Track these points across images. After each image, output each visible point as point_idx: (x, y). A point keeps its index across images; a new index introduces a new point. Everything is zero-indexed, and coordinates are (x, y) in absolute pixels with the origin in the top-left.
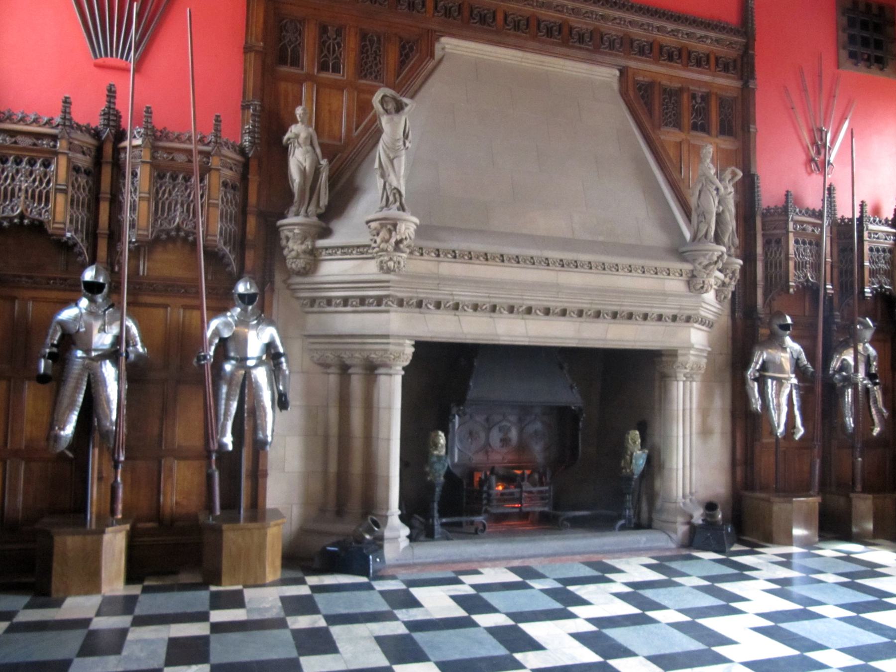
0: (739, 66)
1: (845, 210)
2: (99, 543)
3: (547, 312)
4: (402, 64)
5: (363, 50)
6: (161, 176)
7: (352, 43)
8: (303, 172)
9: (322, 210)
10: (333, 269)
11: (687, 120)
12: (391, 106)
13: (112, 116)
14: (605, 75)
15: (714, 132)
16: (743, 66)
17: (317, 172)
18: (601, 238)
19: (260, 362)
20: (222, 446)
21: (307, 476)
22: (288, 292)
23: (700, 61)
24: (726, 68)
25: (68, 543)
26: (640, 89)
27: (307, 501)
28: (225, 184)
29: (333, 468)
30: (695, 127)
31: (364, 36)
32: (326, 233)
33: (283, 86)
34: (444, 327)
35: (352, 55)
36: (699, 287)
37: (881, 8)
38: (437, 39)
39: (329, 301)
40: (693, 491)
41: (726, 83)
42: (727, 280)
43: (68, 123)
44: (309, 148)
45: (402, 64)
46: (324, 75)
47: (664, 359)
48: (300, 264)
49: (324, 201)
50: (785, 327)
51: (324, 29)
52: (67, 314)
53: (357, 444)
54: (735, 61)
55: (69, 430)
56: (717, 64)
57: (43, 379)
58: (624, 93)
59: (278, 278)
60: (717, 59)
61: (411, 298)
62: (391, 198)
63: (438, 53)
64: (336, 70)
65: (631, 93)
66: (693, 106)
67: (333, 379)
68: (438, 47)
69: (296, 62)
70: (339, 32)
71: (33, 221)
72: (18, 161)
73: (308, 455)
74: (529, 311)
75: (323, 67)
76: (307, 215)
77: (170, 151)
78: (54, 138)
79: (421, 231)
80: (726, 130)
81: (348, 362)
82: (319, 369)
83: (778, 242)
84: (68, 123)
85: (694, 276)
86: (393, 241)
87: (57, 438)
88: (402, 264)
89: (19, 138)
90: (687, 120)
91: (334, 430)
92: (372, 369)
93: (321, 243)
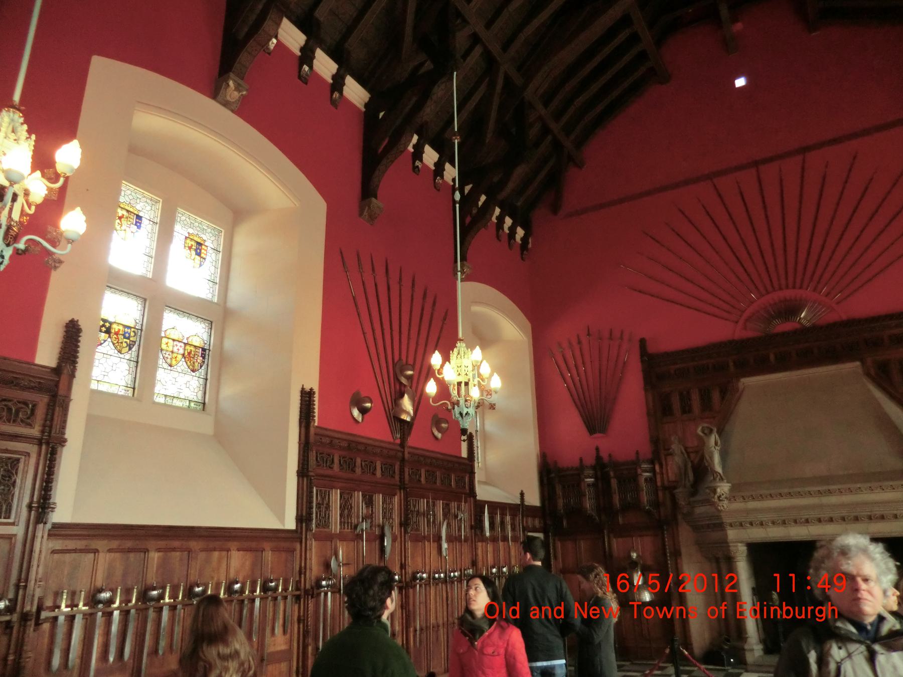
3: (820, 520)
7: (695, 398)
13: (598, 458)
14: (852, 367)
17: (686, 466)
32: (694, 493)
34: (759, 534)
48: (685, 511)
59: (680, 517)
65: (872, 372)
74: (807, 521)
79: (732, 489)
93: (692, 499)
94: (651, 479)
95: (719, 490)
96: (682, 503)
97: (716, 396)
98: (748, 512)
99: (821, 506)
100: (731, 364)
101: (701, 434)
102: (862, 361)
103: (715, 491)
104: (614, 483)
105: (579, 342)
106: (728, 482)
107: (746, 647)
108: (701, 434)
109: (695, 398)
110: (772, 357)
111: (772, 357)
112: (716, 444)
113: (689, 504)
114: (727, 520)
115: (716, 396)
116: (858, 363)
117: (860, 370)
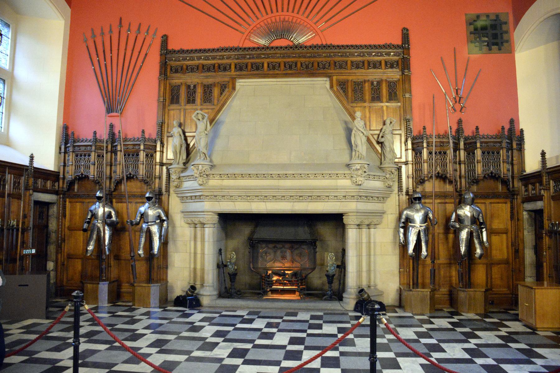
0: (400, 63)
5: (205, 92)
7: (199, 91)
9: (185, 161)
10: (188, 185)
11: (367, 96)
12: (200, 118)
14: (322, 83)
15: (384, 100)
18: (304, 162)
20: (139, 255)
22: (175, 195)
23: (376, 65)
24: (392, 67)
28: (147, 155)
29: (192, 266)
32: (185, 169)
35: (199, 94)
36: (355, 181)
37: (497, 16)
39: (187, 197)
41: (394, 74)
42: (388, 176)
43: (96, 140)
44: (179, 136)
45: (221, 94)
47: (344, 217)
48: (175, 183)
49: (184, 157)
52: (93, 208)
53: (199, 256)
56: (386, 65)
59: (171, 191)
60: (386, 62)
61: (212, 195)
62: (202, 155)
66: (372, 89)
67: (193, 229)
71: (85, 176)
76: (178, 164)
78: (91, 146)
80: (392, 97)
81: (196, 222)
82: (188, 225)
83: (421, 153)
84: (96, 140)
85: (352, 177)
86: (198, 173)
87: (87, 250)
88: (205, 182)
89: (81, 148)
90: (367, 96)
91: (192, 251)
92: (203, 225)
96: (173, 177)
98: (222, 188)
99: (278, 188)
100: (233, 67)
102: (330, 77)
103: (198, 169)
105: (111, 31)
108: (195, 119)
109: (199, 91)
110: (266, 65)
111: (266, 65)
115: (216, 91)
117: (328, 86)
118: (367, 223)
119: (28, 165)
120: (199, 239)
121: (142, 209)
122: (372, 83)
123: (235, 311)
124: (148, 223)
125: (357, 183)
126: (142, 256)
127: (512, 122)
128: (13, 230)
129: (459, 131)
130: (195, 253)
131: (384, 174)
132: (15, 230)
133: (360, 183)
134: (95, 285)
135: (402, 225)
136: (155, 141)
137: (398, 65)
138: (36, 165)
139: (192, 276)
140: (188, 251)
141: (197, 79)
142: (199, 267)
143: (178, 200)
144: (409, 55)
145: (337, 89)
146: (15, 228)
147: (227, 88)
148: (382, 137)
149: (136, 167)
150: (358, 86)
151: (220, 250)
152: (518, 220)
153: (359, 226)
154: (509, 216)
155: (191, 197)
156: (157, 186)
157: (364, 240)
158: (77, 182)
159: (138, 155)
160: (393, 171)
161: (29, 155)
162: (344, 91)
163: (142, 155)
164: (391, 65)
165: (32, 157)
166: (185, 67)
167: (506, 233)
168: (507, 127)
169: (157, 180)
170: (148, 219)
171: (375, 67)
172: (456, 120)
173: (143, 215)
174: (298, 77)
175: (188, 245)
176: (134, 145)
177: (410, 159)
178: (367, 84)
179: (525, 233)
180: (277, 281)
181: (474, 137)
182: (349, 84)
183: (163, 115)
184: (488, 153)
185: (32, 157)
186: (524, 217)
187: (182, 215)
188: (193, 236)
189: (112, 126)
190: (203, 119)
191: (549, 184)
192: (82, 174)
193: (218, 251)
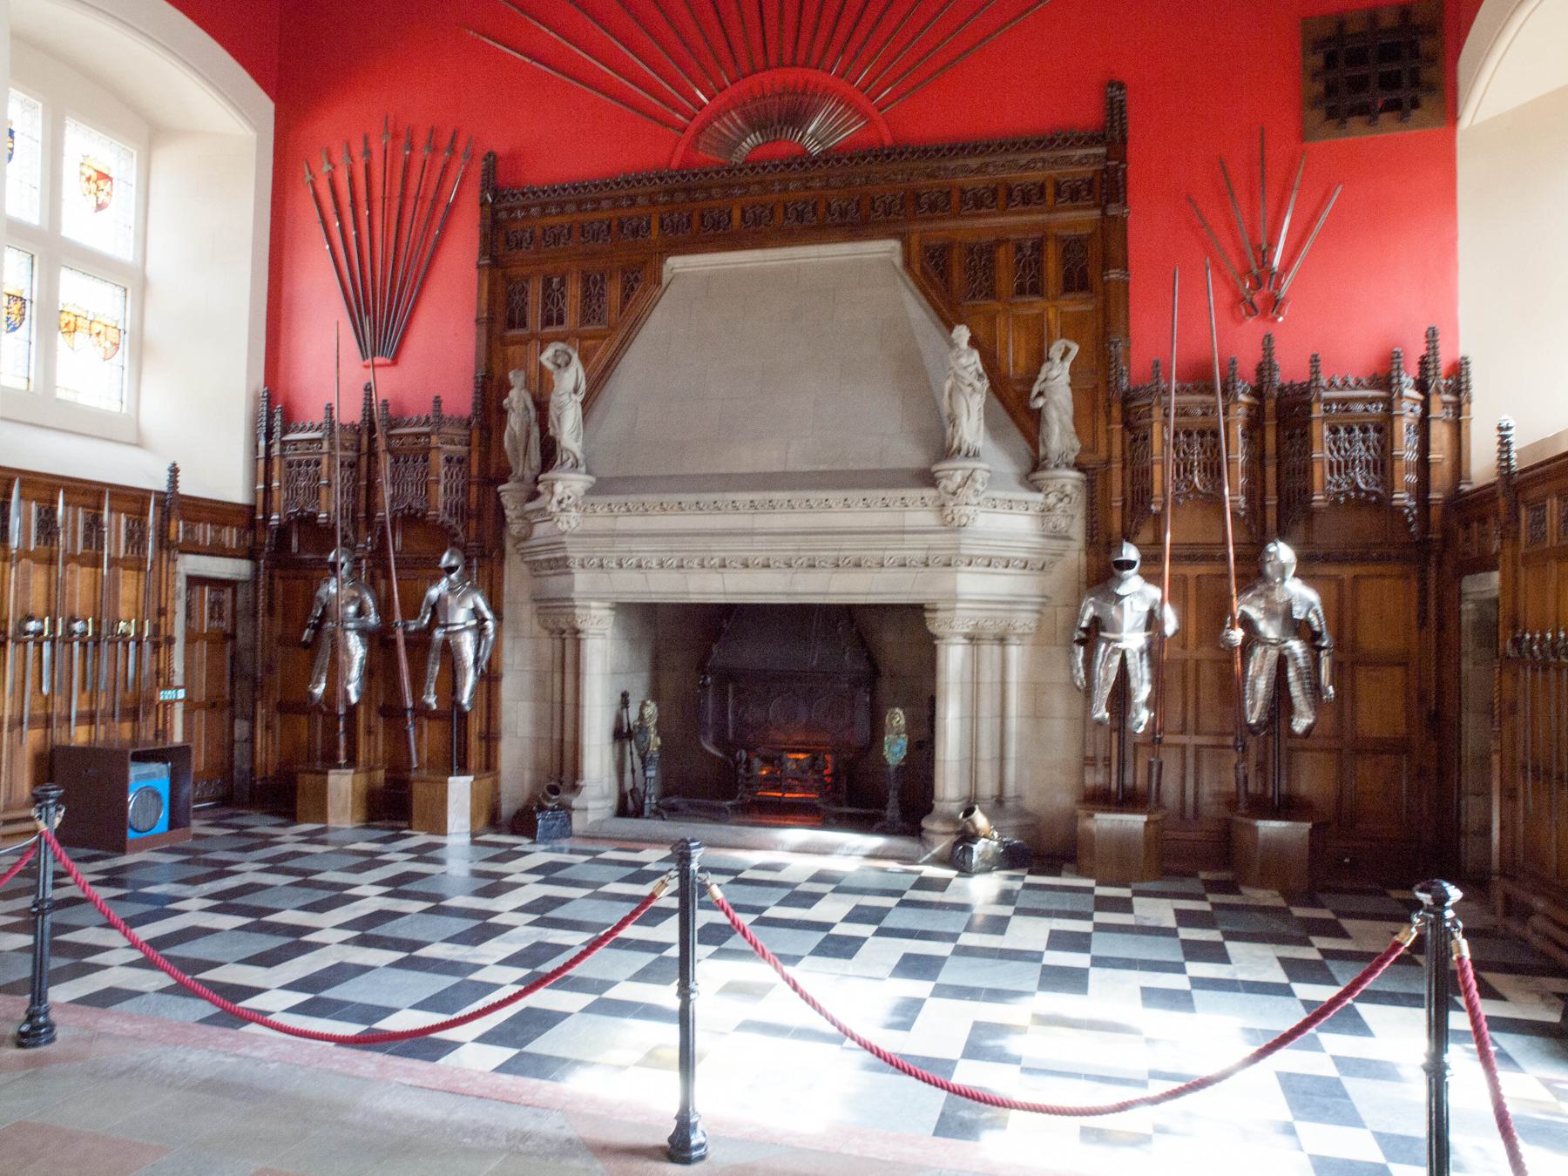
1: (1289, 369)
2: (325, 782)
4: (626, 297)
5: (586, 295)
6: (397, 461)
7: (574, 290)
8: (513, 438)
14: (883, 250)
16: (1108, 188)
19: (467, 629)
20: (428, 706)
21: (537, 741)
23: (1031, 197)
24: (1075, 195)
25: (307, 780)
26: (932, 257)
27: (537, 768)
28: (449, 460)
29: (557, 736)
30: (1021, 291)
31: (586, 280)
33: (511, 350)
38: (662, 261)
39: (540, 562)
40: (1010, 791)
41: (1079, 219)
45: (628, 297)
46: (548, 330)
50: (1130, 565)
51: (548, 283)
53: (569, 710)
54: (1091, 181)
55: (319, 690)
57: (306, 645)
58: (907, 264)
63: (666, 277)
64: (560, 321)
66: (1019, 262)
67: (558, 643)
68: (665, 269)
69: (523, 324)
70: (563, 283)
72: (299, 465)
73: (538, 722)
75: (548, 322)
77: (400, 436)
78: (319, 440)
80: (1076, 281)
82: (546, 633)
91: (557, 697)
94: (460, 461)
95: (559, 488)
97: (614, 292)
100: (655, 224)
101: (549, 366)
104: (385, 463)
106: (588, 472)
107: (575, 803)
110: (736, 214)
111: (736, 214)
112: (576, 391)
113: (523, 517)
114: (575, 553)
115: (614, 292)
116: (894, 245)
117: (898, 260)
118: (992, 629)
119: (165, 489)
120: (569, 670)
121: (434, 593)
122: (1019, 248)
123: (637, 851)
124: (446, 626)
125: (956, 523)
126: (435, 707)
127: (1432, 336)
128: (126, 644)
129: (1264, 369)
130: (563, 702)
131: (1040, 497)
132: (132, 644)
133: (964, 520)
134: (319, 778)
135: (1078, 635)
136: (469, 423)
137: (1090, 192)
138: (184, 489)
139: (556, 760)
140: (548, 697)
141: (569, 263)
142: (568, 737)
143: (524, 568)
144: (1124, 160)
145: (922, 267)
146: (47, 639)
147: (640, 280)
148: (1040, 394)
149: (426, 486)
150: (982, 256)
151: (625, 696)
152: (1441, 627)
153: (973, 639)
154: (1414, 614)
155: (548, 560)
156: (472, 534)
157: (989, 675)
158: (295, 528)
159: (426, 460)
160: (1069, 489)
161: (168, 465)
162: (941, 274)
163: (438, 459)
164: (1073, 194)
165: (174, 471)
166: (539, 232)
167: (1406, 664)
168: (1420, 349)
169: (473, 524)
170: (446, 619)
171: (1026, 200)
172: (1259, 338)
173: (434, 608)
174: (819, 241)
175: (549, 683)
176: (418, 436)
177: (1117, 450)
178: (1002, 250)
179: (1464, 667)
180: (766, 778)
181: (1305, 389)
182: (956, 254)
183: (489, 359)
184: (1350, 431)
185: (174, 471)
186: (1464, 618)
187: (535, 605)
188: (558, 662)
189: (368, 390)
190: (567, 364)
191: (1518, 520)
192: (302, 511)
193: (619, 697)
